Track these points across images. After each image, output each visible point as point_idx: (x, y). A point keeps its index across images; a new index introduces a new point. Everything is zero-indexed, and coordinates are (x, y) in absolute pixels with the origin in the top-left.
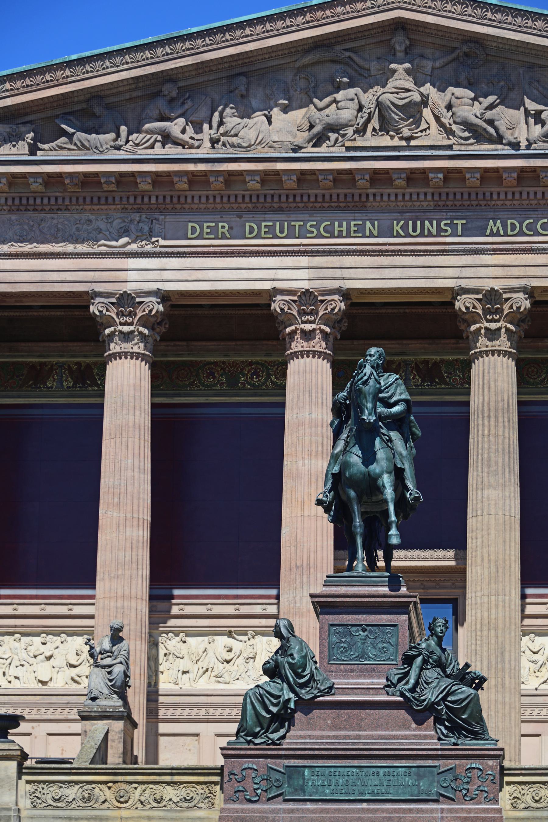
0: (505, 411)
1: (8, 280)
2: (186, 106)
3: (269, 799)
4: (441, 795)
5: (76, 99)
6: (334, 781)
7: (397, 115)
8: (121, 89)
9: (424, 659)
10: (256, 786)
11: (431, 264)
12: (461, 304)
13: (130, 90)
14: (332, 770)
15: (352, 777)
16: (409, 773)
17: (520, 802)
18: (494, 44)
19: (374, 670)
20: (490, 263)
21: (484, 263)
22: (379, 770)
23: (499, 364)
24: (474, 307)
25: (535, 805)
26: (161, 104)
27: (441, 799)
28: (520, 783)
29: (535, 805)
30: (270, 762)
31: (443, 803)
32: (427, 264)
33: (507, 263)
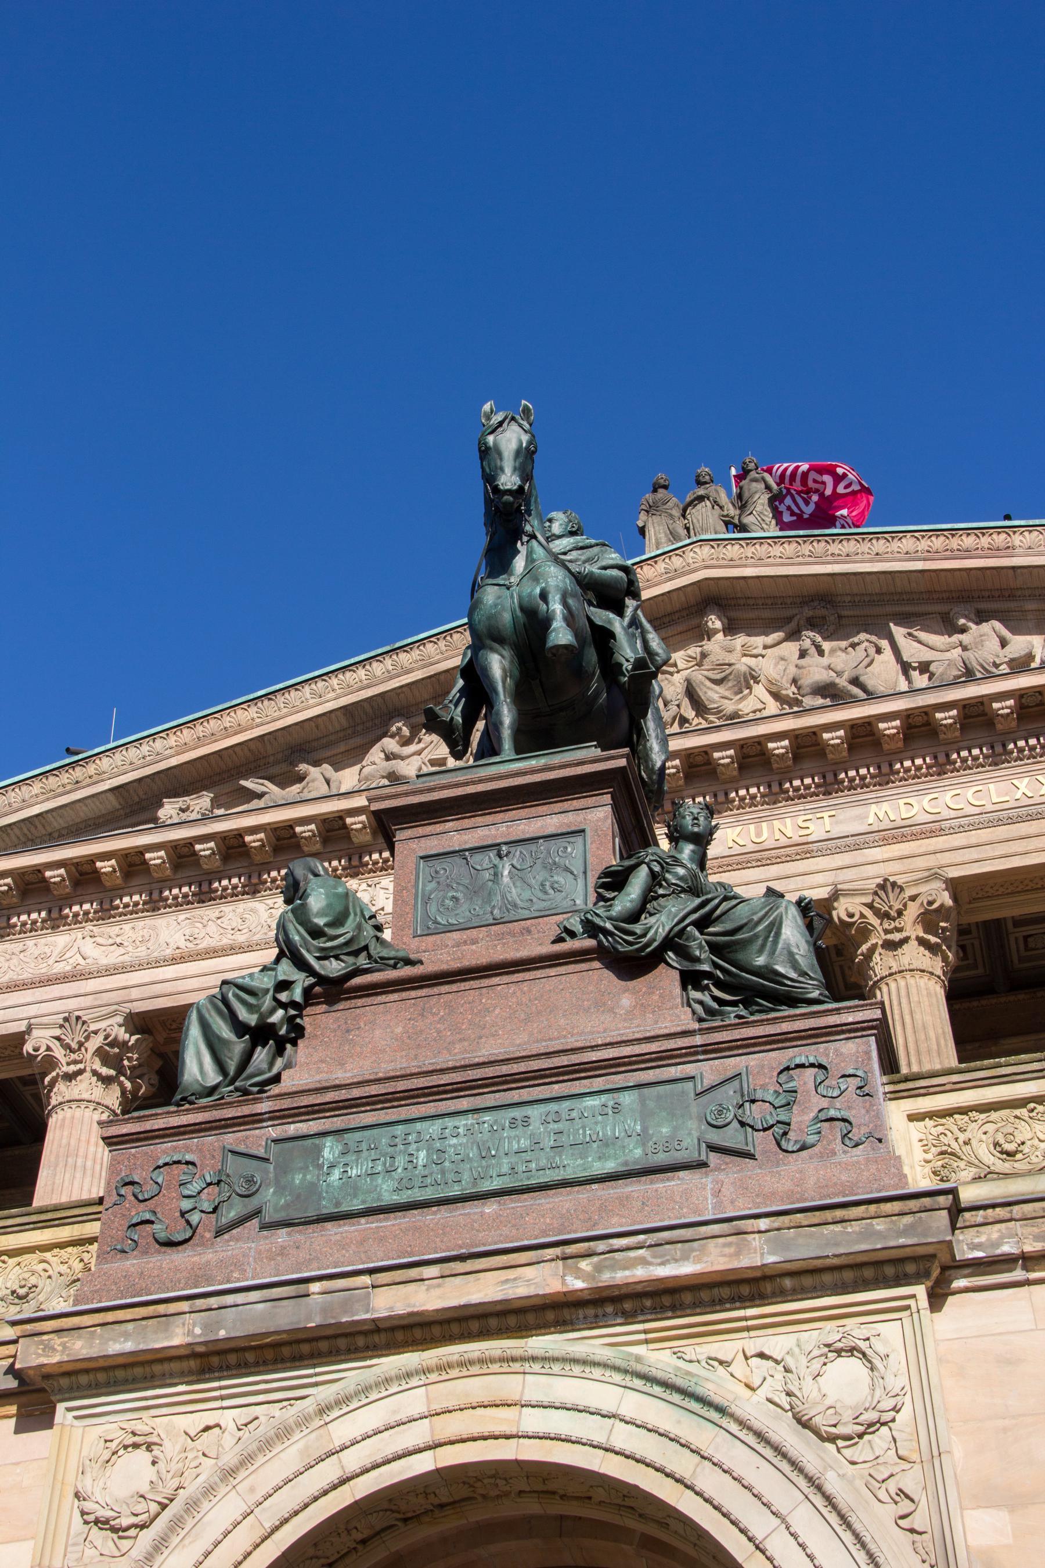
0: (935, 1054)
1: (168, 992)
2: (422, 745)
3: (219, 1233)
4: (713, 1148)
5: (272, 759)
6: (401, 1161)
7: (717, 693)
8: (332, 738)
9: (653, 874)
10: (186, 1204)
11: (789, 872)
12: (841, 911)
13: (345, 738)
14: (399, 1130)
15: (454, 1141)
16: (617, 1109)
17: (962, 1164)
18: (849, 598)
19: (529, 931)
20: (879, 858)
21: (870, 859)
22: (528, 1111)
23: (913, 991)
24: (862, 916)
25: (1006, 1167)
26: (390, 744)
27: (714, 1158)
28: (949, 1113)
29: (1006, 1167)
30: (231, 1139)
31: (718, 1169)
32: (783, 874)
33: (906, 853)
